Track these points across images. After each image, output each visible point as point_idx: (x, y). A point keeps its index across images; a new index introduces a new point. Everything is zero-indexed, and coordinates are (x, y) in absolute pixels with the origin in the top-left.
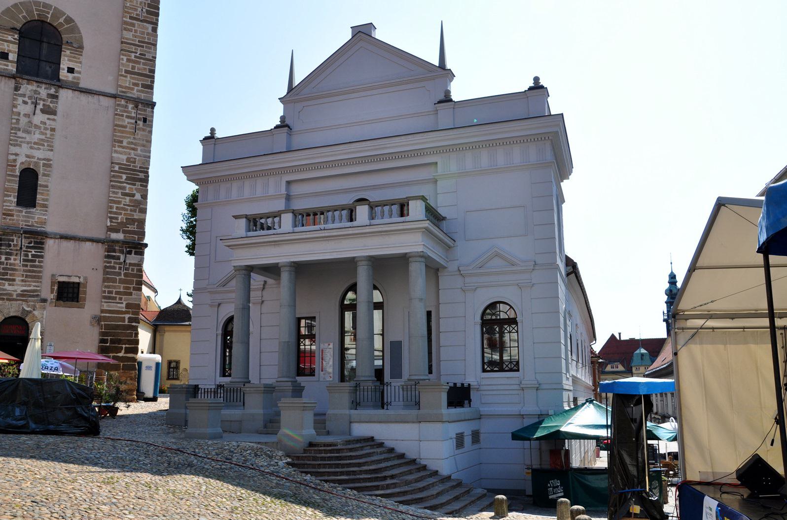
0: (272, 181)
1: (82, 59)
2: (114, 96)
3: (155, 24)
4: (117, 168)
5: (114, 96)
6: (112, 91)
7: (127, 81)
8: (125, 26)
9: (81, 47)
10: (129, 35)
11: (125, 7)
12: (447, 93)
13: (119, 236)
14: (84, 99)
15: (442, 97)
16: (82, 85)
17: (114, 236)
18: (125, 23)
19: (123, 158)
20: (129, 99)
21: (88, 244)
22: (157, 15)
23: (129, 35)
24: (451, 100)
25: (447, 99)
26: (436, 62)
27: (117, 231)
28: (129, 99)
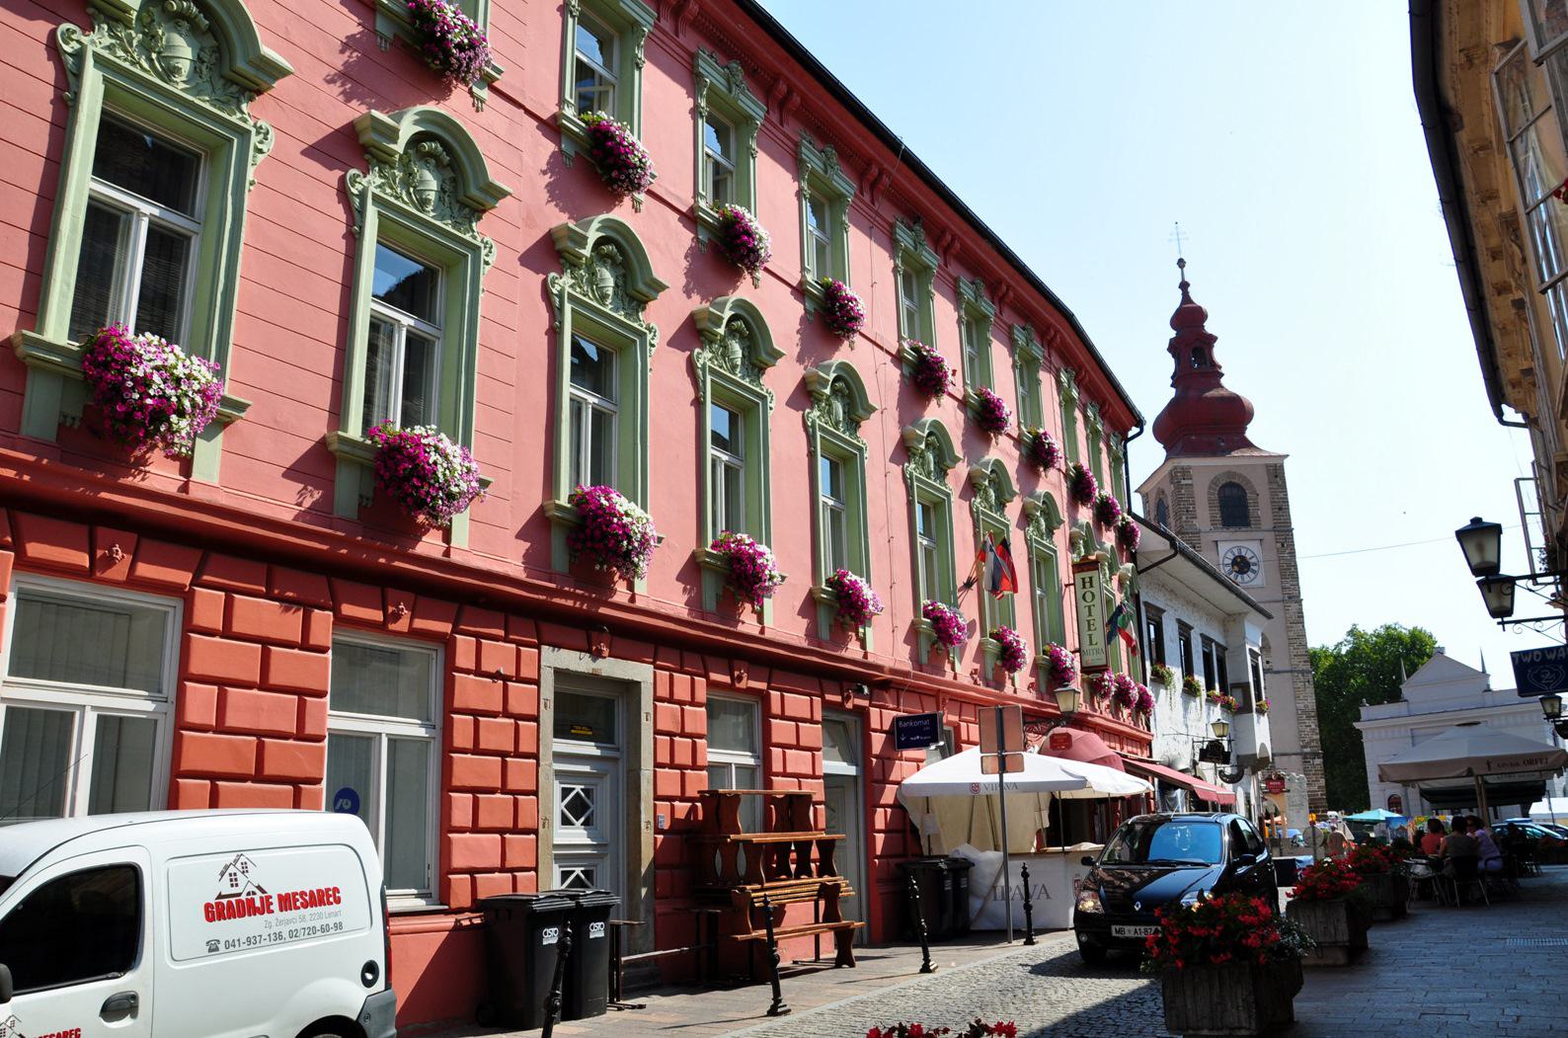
0: (1403, 729)
1: (1272, 654)
2: (1291, 671)
3: (1303, 623)
4: (1300, 712)
5: (1291, 671)
6: (1288, 668)
7: (1295, 661)
8: (1288, 629)
9: (1270, 648)
10: (1291, 634)
11: (1286, 617)
12: (1488, 685)
13: (1308, 750)
14: (1277, 676)
15: (1486, 688)
16: (1275, 669)
17: (1306, 750)
18: (1288, 627)
19: (1301, 706)
20: (1299, 672)
21: (1294, 757)
22: (1303, 617)
23: (1291, 634)
24: (1490, 690)
25: (1488, 690)
26: (1481, 670)
27: (1305, 747)
28: (1299, 672)
